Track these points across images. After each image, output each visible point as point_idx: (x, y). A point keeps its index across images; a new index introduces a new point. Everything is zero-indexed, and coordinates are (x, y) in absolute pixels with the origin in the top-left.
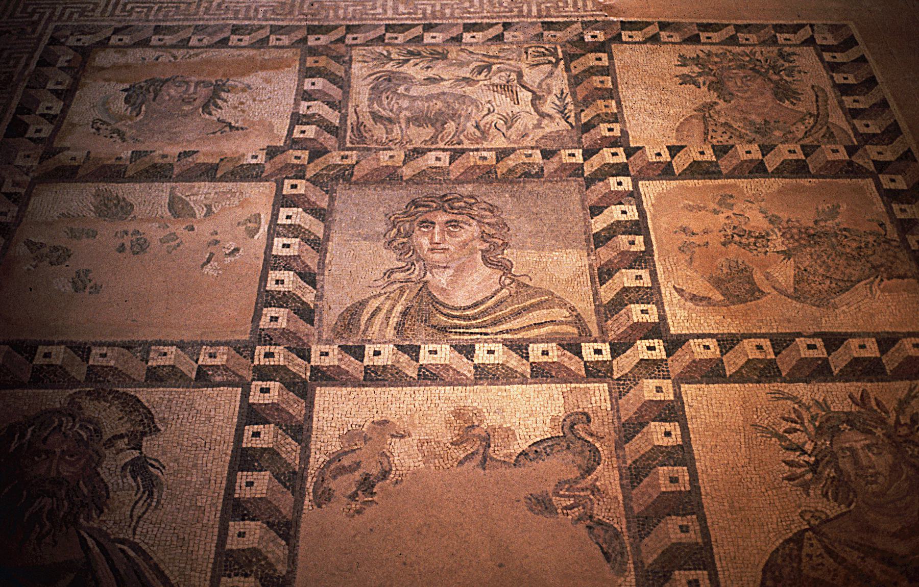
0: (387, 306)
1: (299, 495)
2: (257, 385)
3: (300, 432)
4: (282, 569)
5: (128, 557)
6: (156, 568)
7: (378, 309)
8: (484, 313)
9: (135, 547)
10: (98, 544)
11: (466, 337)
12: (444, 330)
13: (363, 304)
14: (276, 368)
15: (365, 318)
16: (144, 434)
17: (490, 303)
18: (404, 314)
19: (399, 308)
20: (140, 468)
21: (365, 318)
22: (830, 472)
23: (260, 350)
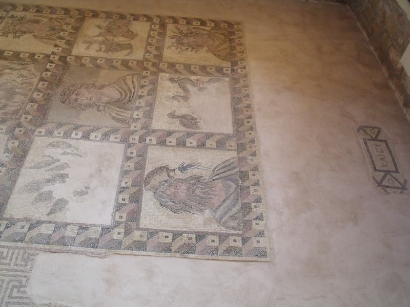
0: (116, 112)
1: (194, 133)
2: (148, 142)
3: (170, 133)
4: (223, 136)
5: (219, 169)
6: (223, 163)
7: (117, 114)
8: (125, 91)
9: (217, 167)
10: (215, 176)
11: (135, 96)
12: (130, 101)
13: (113, 118)
14: (140, 138)
15: (120, 117)
16: (168, 169)
17: (121, 90)
18: (120, 108)
19: (118, 109)
20: (183, 169)
21: (120, 117)
22: (195, 46)
23: (131, 141)
